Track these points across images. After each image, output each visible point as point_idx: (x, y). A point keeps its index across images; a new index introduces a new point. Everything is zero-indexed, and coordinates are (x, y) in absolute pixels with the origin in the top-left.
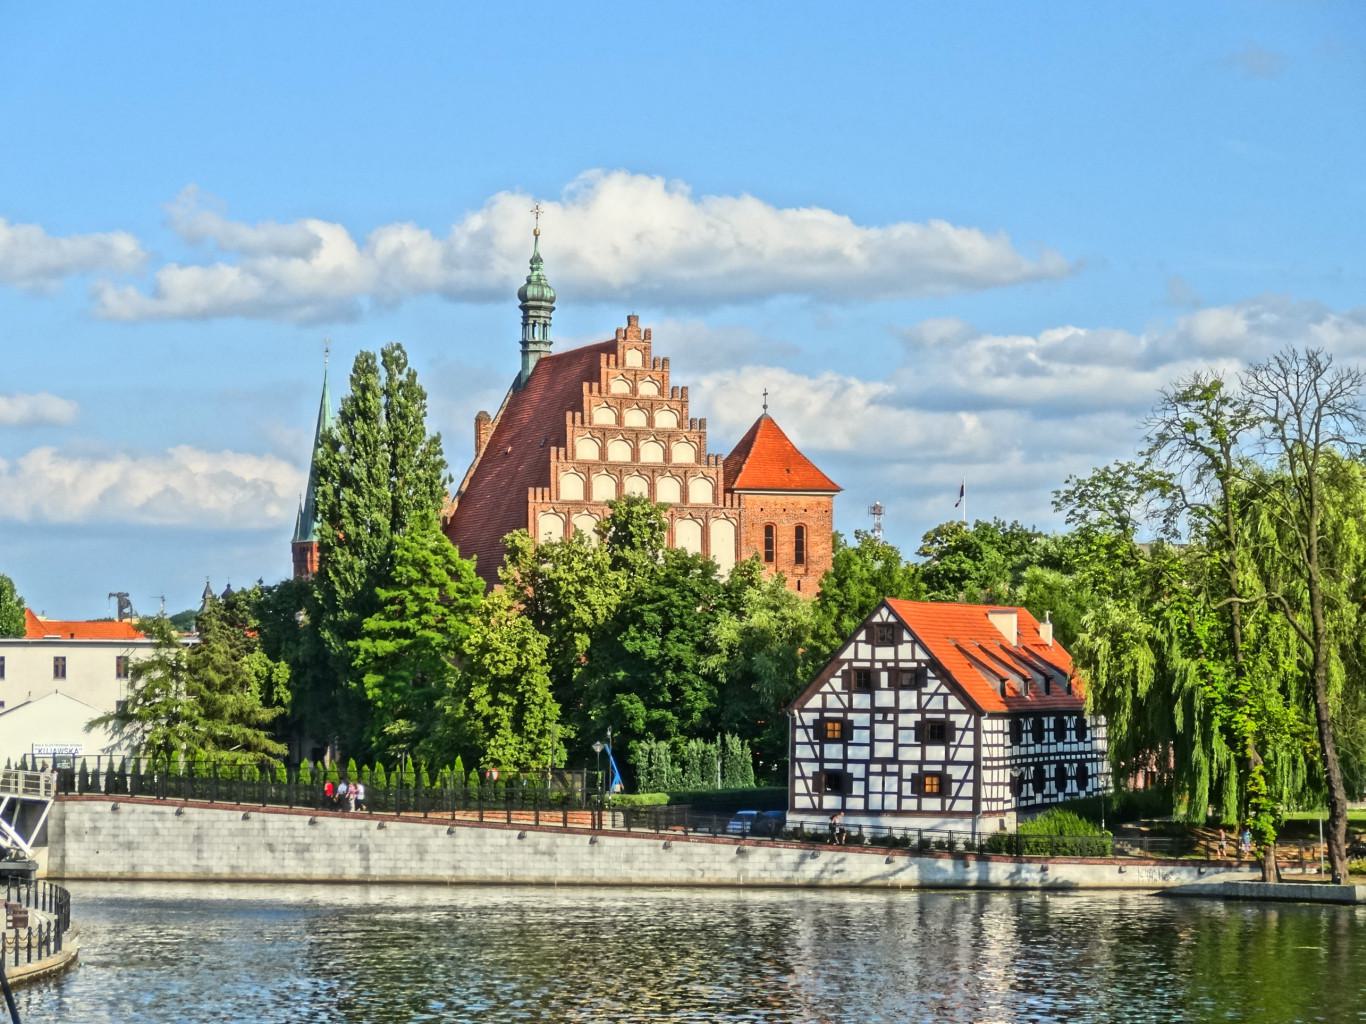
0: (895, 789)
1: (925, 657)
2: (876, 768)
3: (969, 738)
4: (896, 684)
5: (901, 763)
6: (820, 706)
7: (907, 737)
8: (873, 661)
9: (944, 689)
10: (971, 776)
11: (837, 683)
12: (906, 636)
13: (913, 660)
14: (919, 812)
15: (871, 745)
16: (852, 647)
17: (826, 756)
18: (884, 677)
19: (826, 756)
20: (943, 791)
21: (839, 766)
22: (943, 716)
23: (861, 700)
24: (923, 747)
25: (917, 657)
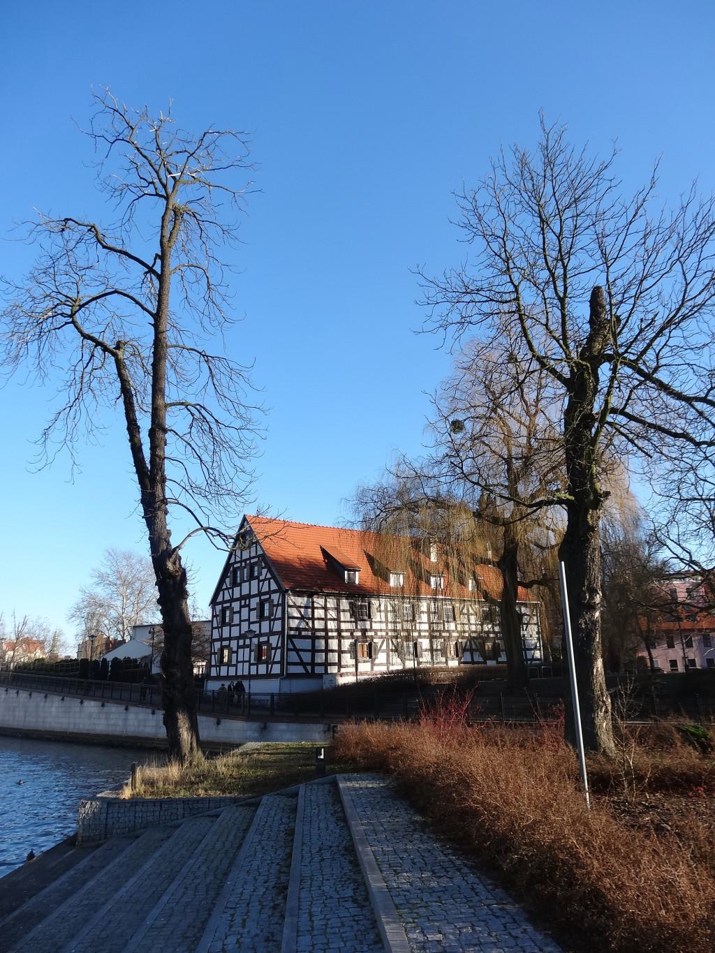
2: (241, 642)
4: (251, 577)
7: (254, 617)
9: (269, 576)
14: (258, 676)
23: (237, 590)
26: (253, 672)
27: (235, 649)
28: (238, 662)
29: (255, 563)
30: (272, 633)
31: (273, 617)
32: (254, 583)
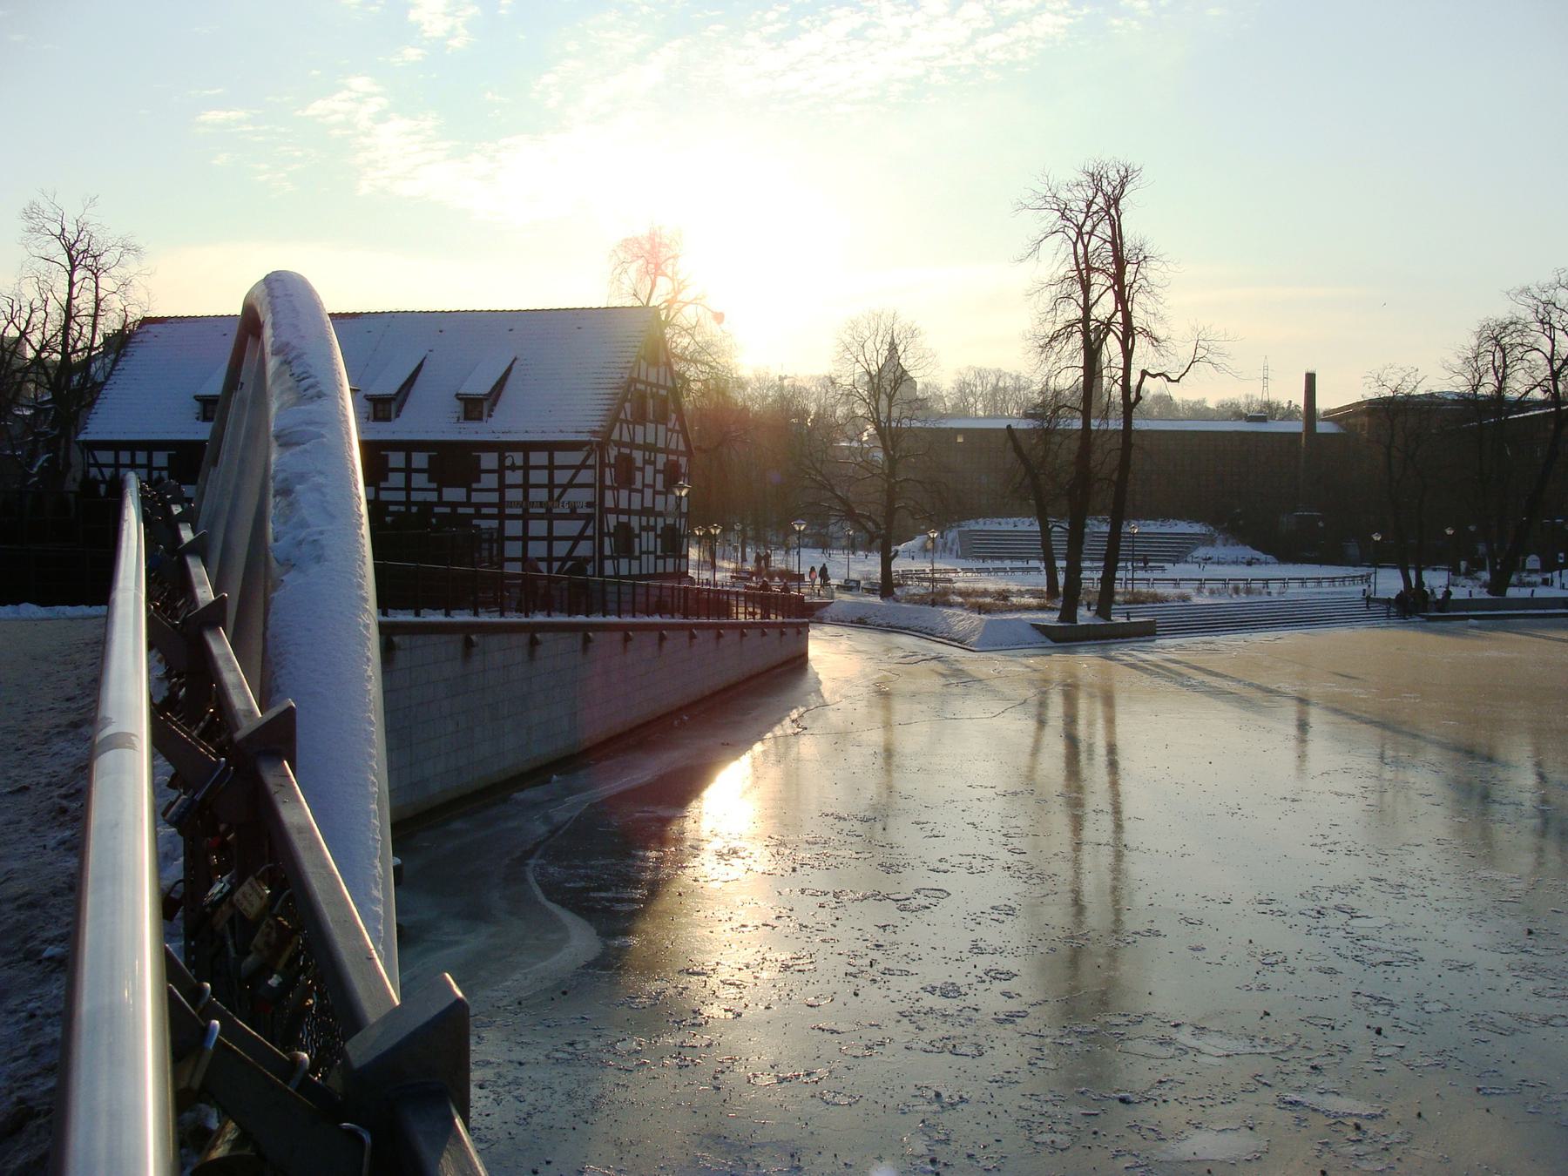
4: (656, 422)
26: (660, 570)
27: (637, 531)
28: (641, 553)
32: (661, 428)
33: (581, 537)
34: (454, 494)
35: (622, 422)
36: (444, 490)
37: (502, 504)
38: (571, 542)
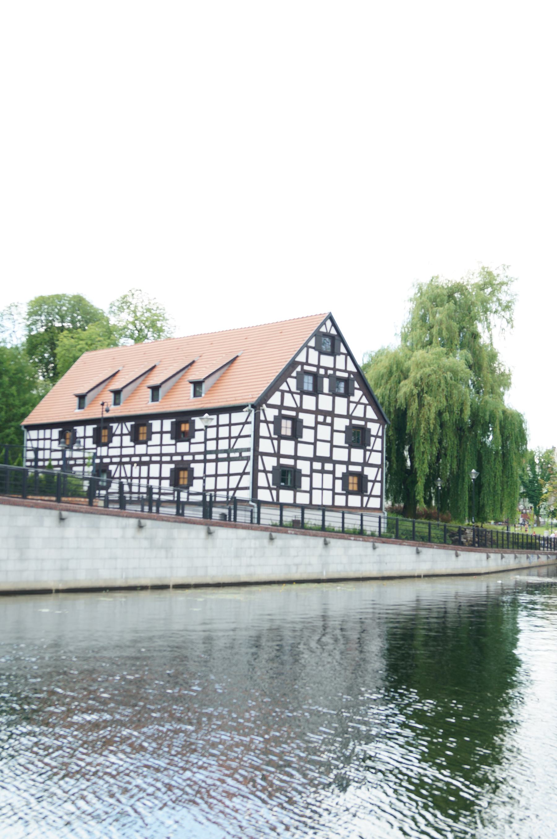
0: (331, 487)
1: (355, 370)
2: (317, 466)
3: (378, 444)
4: (334, 394)
5: (335, 463)
6: (279, 403)
7: (340, 439)
8: (318, 367)
9: (364, 400)
10: (379, 478)
11: (292, 383)
12: (343, 350)
13: (345, 371)
15: (314, 444)
16: (305, 351)
17: (282, 452)
18: (326, 381)
19: (282, 452)
20: (361, 490)
21: (291, 462)
22: (362, 423)
23: (309, 402)
24: (349, 448)
25: (348, 369)
28: (312, 488)
29: (340, 379)
30: (365, 464)
31: (368, 448)
33: (244, 473)
34: (183, 447)
35: (283, 392)
36: (179, 444)
37: (206, 453)
38: (239, 477)
